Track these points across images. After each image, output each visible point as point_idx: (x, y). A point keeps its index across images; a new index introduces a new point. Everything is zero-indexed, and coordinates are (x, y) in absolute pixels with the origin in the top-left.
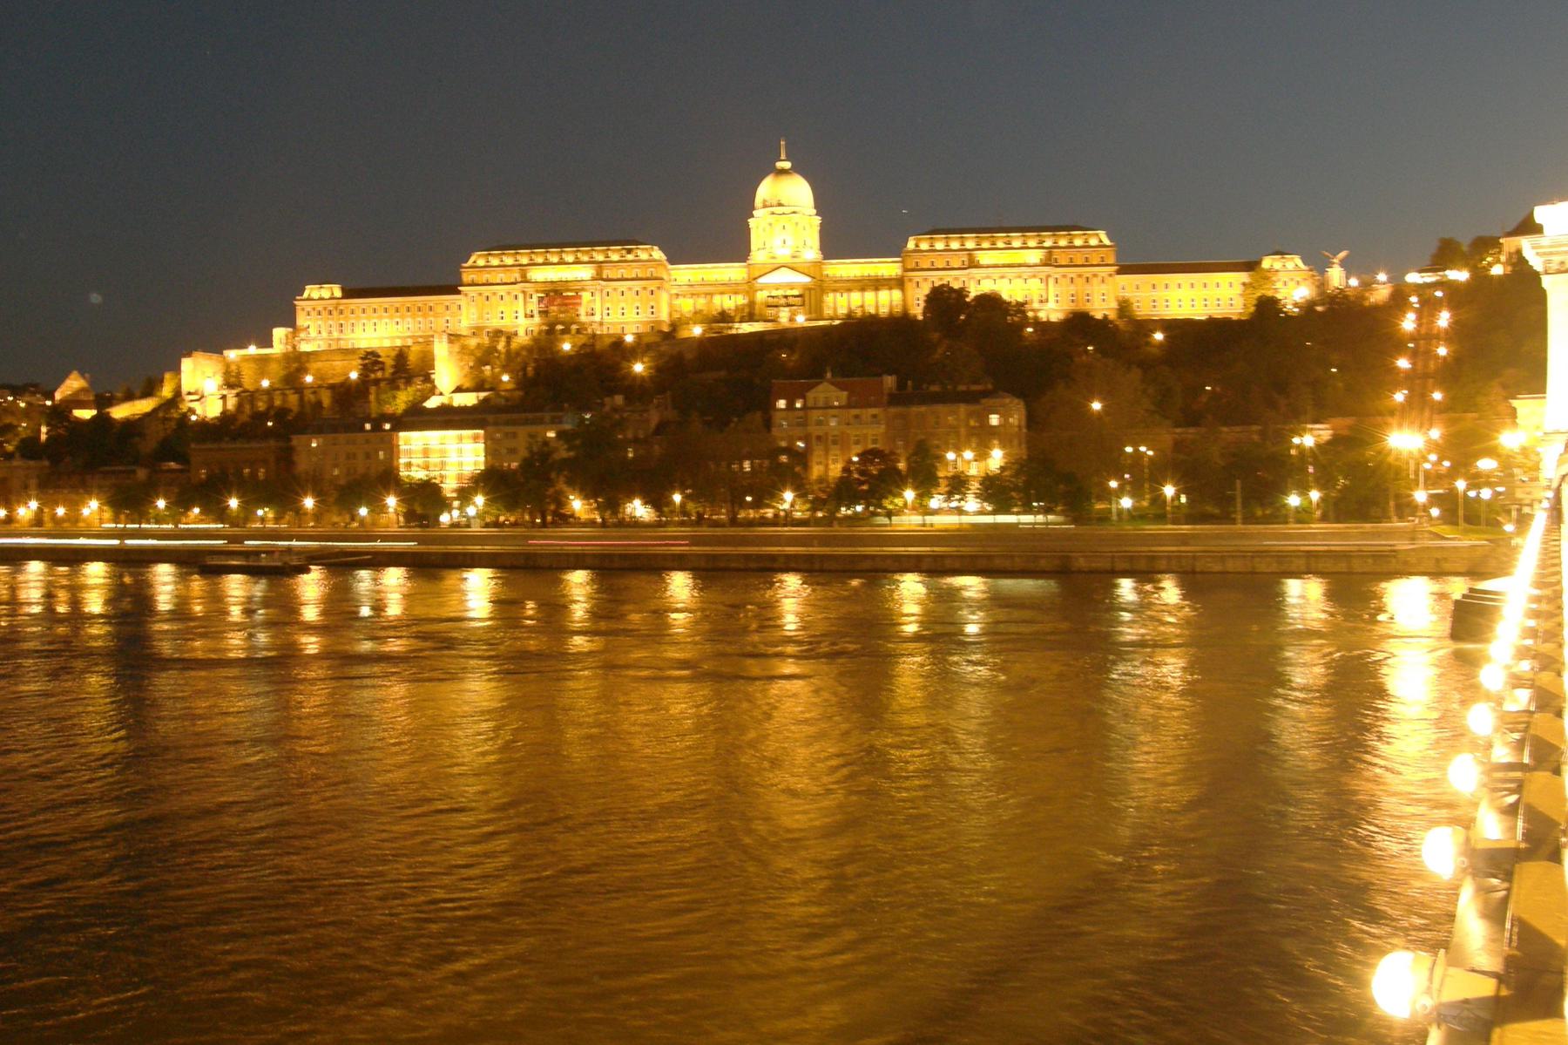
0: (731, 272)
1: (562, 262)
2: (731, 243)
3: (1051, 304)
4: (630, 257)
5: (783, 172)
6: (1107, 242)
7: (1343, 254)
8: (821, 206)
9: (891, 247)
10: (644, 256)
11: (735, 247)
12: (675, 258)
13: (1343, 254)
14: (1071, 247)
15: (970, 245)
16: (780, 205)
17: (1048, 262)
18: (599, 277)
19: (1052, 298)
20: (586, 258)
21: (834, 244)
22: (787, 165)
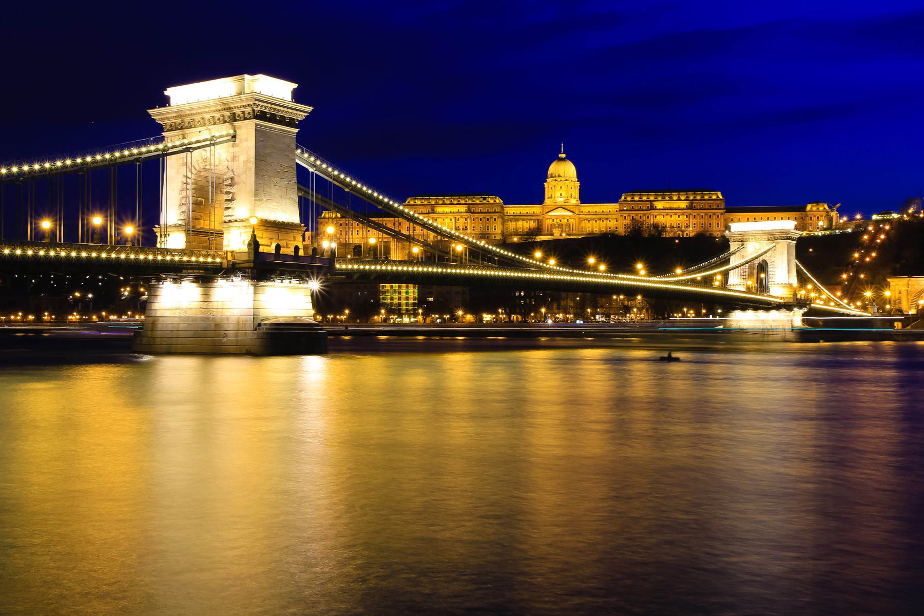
0: (535, 209)
2: (534, 193)
5: (562, 159)
7: (838, 205)
9: (614, 199)
10: (492, 201)
11: (538, 197)
12: (508, 201)
13: (838, 205)
14: (702, 199)
15: (652, 198)
17: (690, 207)
18: (469, 211)
20: (463, 202)
21: (586, 197)
22: (564, 156)
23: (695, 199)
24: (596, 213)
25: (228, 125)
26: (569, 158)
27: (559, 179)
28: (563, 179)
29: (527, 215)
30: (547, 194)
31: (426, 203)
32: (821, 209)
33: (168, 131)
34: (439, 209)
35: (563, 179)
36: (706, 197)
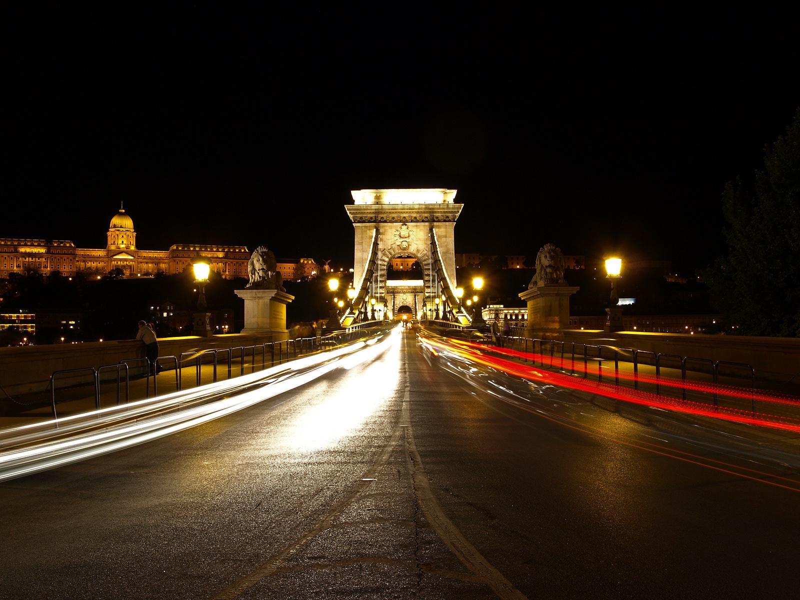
0: (100, 253)
1: (32, 245)
3: (227, 273)
4: (62, 245)
5: (122, 214)
6: (247, 251)
7: (329, 261)
8: (136, 228)
11: (102, 243)
12: (80, 245)
13: (329, 261)
14: (234, 251)
16: (121, 227)
18: (48, 252)
19: (227, 271)
21: (140, 245)
22: (124, 211)
23: (229, 251)
24: (150, 258)
25: (427, 224)
26: (128, 213)
27: (121, 229)
28: (124, 230)
29: (94, 257)
30: (110, 241)
31: (9, 243)
32: (310, 262)
33: (359, 222)
34: (22, 250)
35: (124, 230)
36: (237, 250)
